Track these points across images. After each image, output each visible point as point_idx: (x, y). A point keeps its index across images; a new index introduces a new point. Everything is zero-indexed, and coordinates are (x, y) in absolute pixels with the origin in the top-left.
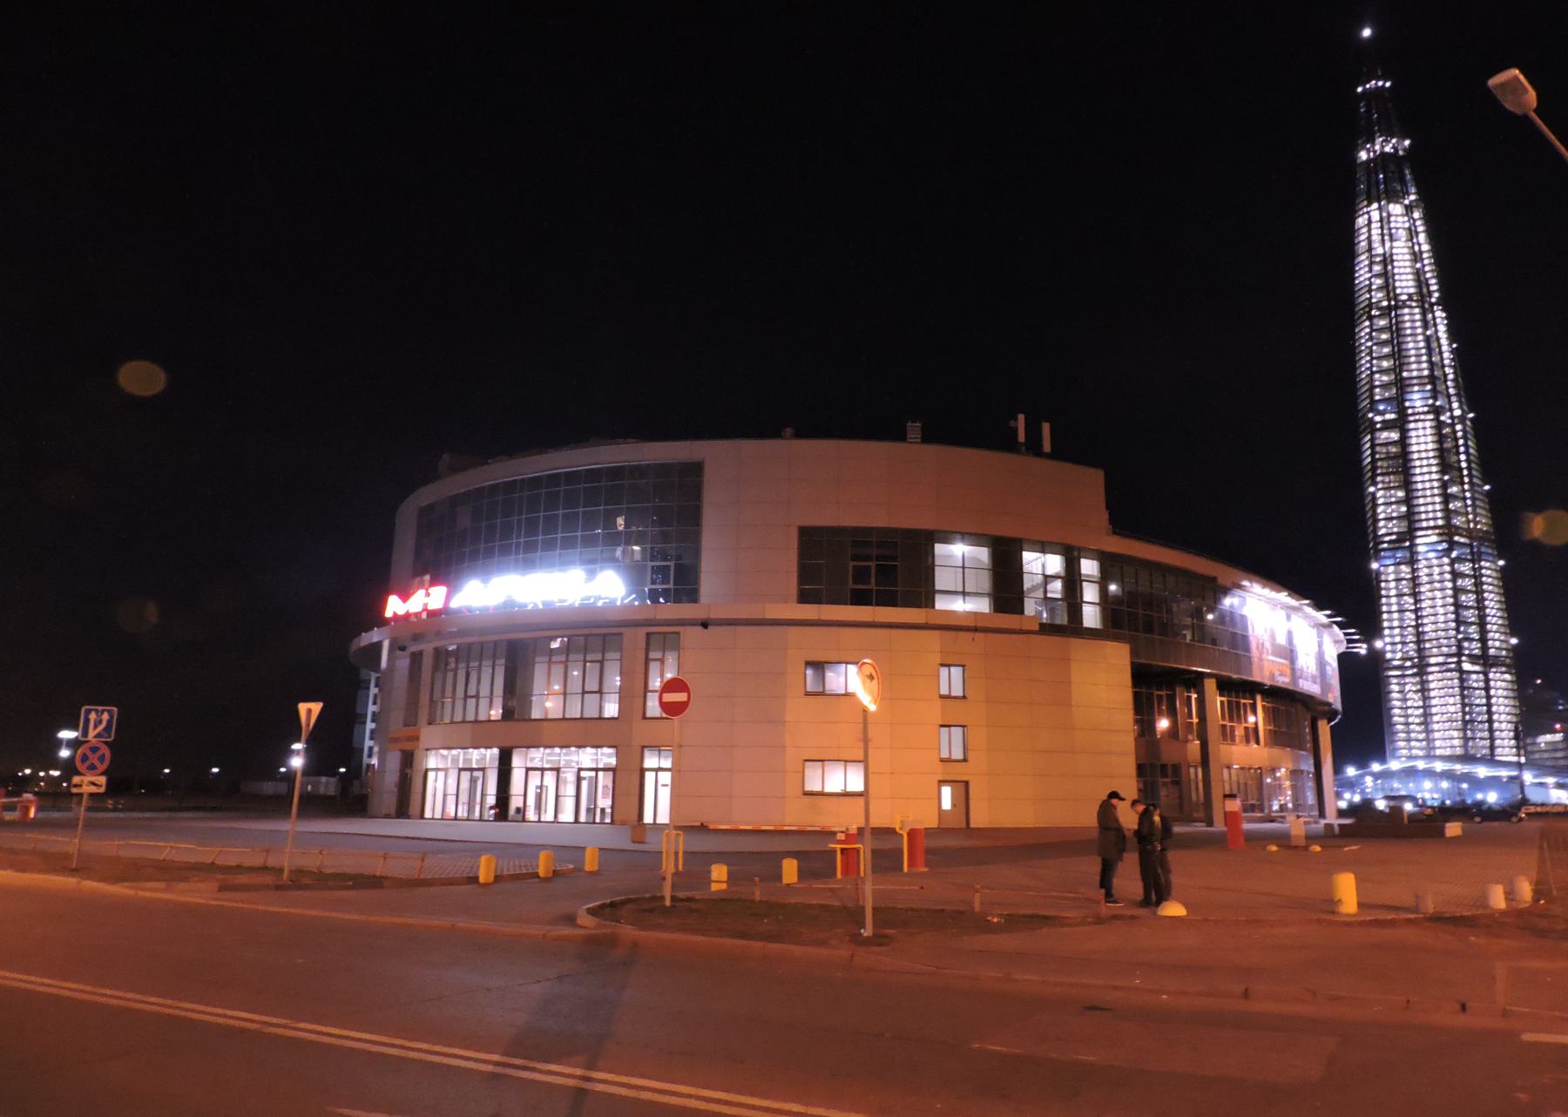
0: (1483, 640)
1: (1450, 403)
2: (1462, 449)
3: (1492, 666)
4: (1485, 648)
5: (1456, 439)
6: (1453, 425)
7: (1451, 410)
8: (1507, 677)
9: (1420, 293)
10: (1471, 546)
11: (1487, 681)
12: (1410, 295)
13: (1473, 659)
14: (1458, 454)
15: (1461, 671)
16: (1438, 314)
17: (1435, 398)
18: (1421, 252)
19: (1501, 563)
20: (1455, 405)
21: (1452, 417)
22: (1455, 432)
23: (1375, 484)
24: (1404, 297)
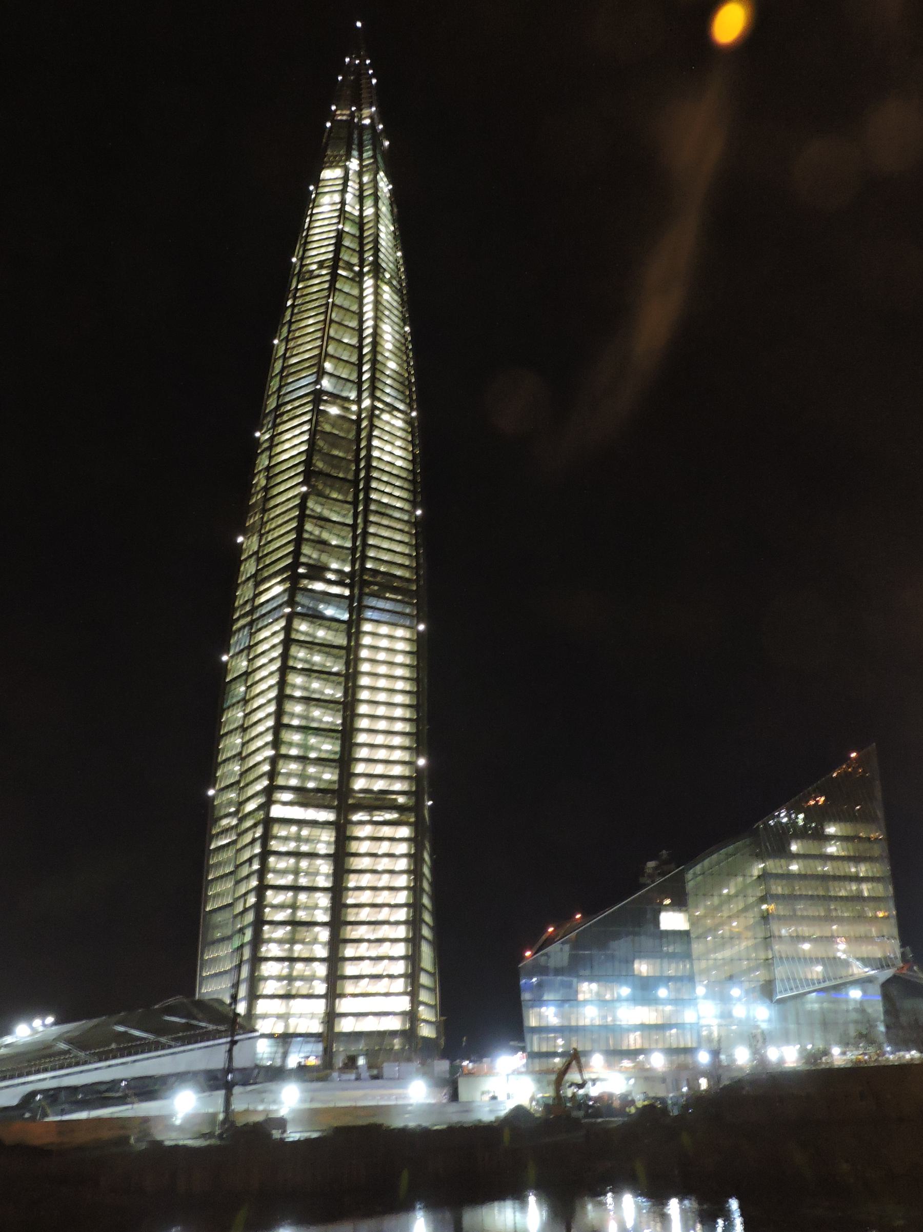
0: (344, 762)
1: (360, 393)
2: (363, 453)
3: (358, 807)
4: (346, 775)
5: (358, 440)
6: (359, 420)
7: (359, 401)
8: (404, 832)
9: (336, 259)
10: (351, 598)
11: (343, 839)
12: (321, 264)
13: (305, 797)
14: (357, 460)
15: (268, 823)
16: (369, 282)
17: (317, 382)
18: (361, 216)
19: (421, 627)
20: (365, 394)
21: (360, 411)
22: (359, 430)
23: (244, 531)
24: (314, 267)
